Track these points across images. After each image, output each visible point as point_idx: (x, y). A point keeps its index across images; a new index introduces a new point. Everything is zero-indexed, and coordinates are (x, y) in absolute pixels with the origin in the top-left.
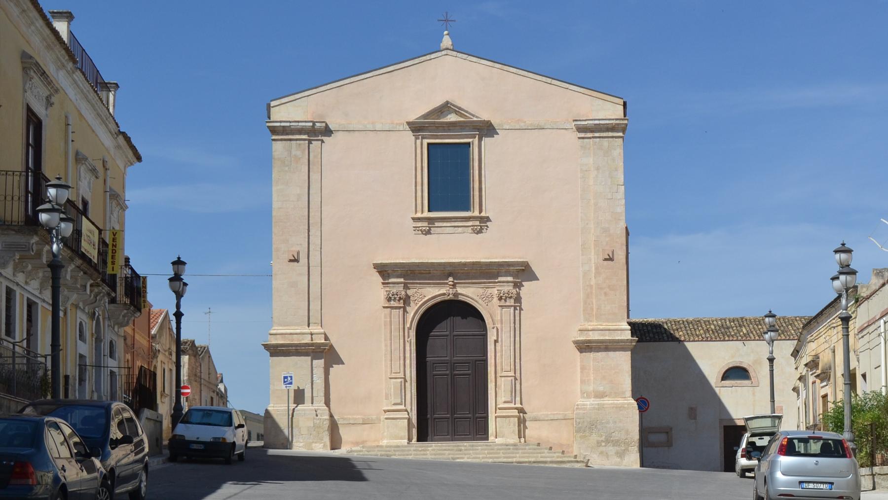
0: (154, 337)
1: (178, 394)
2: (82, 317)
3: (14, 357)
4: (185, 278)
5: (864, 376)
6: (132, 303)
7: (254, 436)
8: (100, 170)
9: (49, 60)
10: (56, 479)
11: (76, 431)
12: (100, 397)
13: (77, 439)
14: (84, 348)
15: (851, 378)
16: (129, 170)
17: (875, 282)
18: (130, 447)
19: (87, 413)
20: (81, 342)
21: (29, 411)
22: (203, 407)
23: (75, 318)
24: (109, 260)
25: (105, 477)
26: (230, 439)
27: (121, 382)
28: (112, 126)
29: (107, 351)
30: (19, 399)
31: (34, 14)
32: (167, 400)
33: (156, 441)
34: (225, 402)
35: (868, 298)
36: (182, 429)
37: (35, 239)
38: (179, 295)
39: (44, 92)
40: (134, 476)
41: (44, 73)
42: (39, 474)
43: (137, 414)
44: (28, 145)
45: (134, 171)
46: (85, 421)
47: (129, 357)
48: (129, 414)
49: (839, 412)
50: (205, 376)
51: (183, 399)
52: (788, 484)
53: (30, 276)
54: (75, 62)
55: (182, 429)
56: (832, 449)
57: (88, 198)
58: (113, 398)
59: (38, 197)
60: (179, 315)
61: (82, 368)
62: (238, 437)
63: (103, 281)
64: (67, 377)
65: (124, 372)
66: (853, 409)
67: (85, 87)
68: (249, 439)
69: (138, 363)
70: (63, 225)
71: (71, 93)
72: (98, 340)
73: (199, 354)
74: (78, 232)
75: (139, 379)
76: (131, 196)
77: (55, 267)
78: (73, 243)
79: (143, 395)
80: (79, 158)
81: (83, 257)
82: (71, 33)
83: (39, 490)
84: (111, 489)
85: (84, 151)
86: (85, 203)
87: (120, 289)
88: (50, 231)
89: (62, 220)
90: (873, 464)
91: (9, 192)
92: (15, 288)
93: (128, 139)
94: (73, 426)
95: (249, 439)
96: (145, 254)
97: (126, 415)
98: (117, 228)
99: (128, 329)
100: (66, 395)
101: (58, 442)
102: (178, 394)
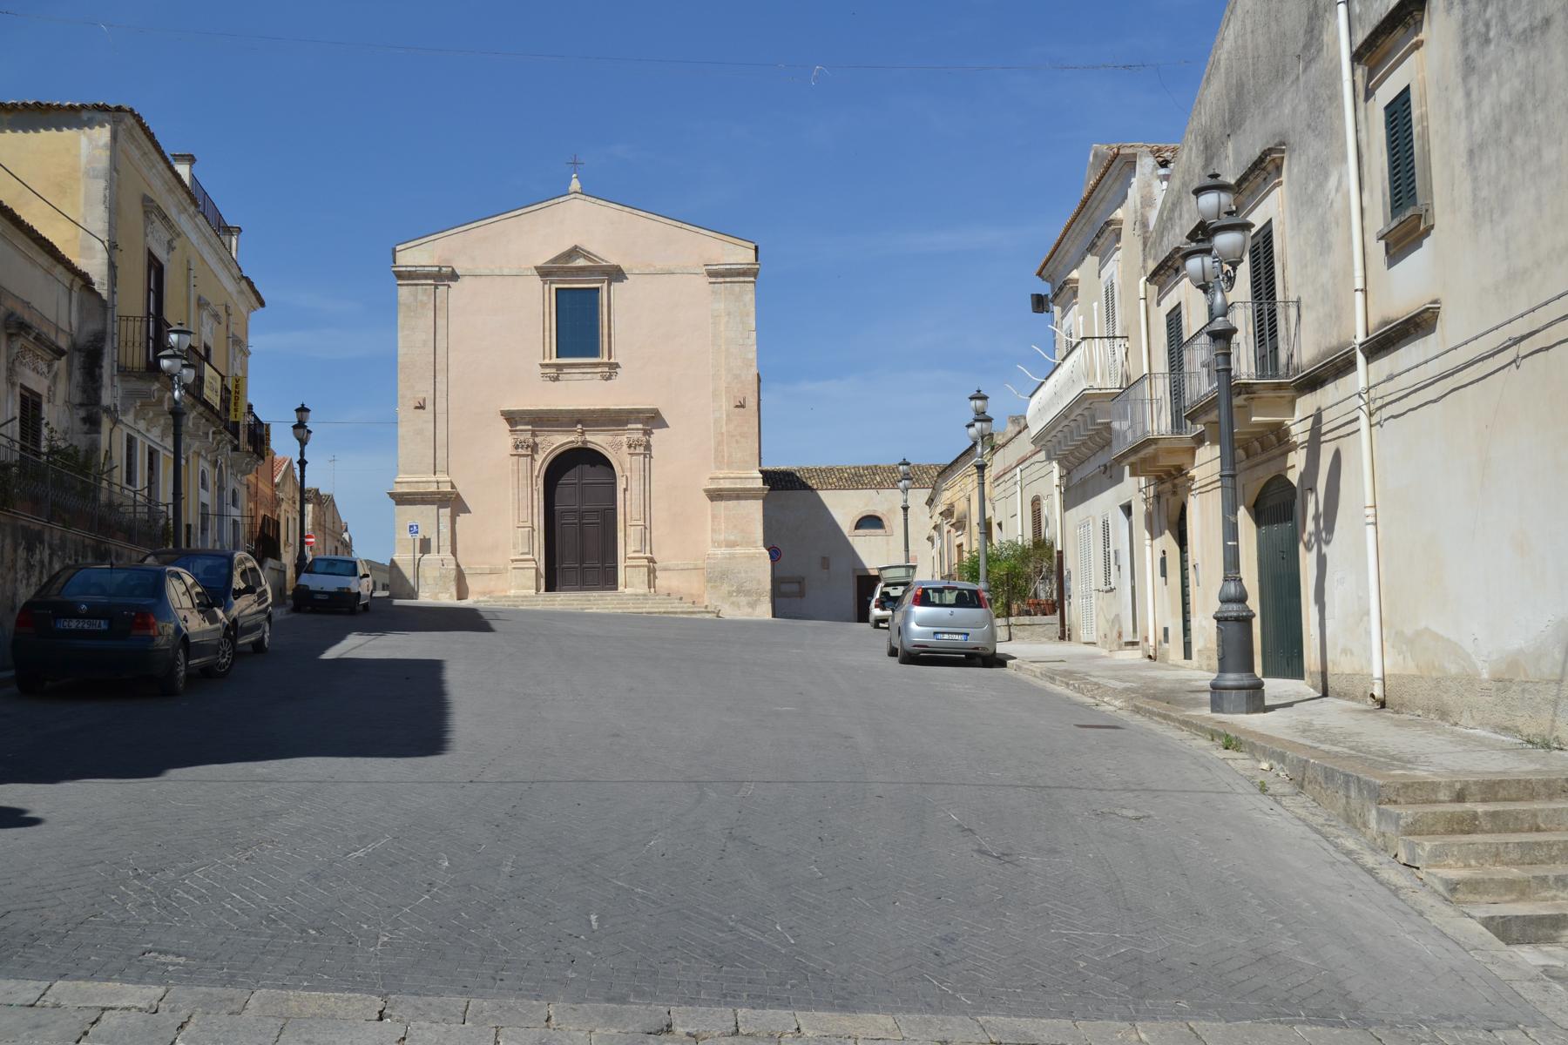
0: (277, 485)
1: (302, 544)
2: (204, 465)
3: (135, 506)
4: (309, 425)
5: (1000, 525)
6: (255, 451)
7: (379, 586)
8: (221, 317)
9: (171, 204)
10: (178, 630)
11: (199, 580)
12: (222, 546)
13: (199, 589)
14: (207, 497)
15: (986, 528)
16: (252, 315)
17: (1011, 429)
18: (254, 597)
19: (209, 562)
20: (204, 491)
21: (150, 560)
22: (328, 556)
23: (197, 466)
24: (232, 407)
25: (227, 628)
26: (354, 588)
27: (243, 531)
28: (235, 271)
29: (230, 500)
30: (142, 549)
31: (155, 156)
32: (290, 549)
33: (279, 591)
34: (350, 553)
35: (1004, 446)
36: (305, 579)
37: (156, 386)
38: (303, 443)
39: (166, 236)
40: (257, 627)
41: (165, 217)
42: (161, 624)
43: (261, 563)
44: (149, 289)
45: (257, 317)
46: (207, 570)
47: (252, 505)
48: (252, 563)
49: (974, 562)
50: (329, 525)
51: (307, 548)
52: (922, 635)
53: (151, 424)
54: (197, 206)
55: (305, 579)
56: (967, 600)
57: (210, 343)
58: (236, 547)
59: (160, 343)
60: (302, 463)
61: (205, 517)
62: (363, 587)
63: (226, 428)
64: (188, 526)
65: (247, 521)
66: (988, 558)
67: (208, 231)
68: (375, 589)
69: (262, 512)
70: (185, 371)
71: (193, 237)
72: (221, 488)
73: (324, 502)
74: (200, 379)
75: (262, 528)
76: (255, 342)
77: (177, 414)
78: (195, 390)
79: (266, 544)
80: (202, 304)
81: (206, 404)
82: (192, 176)
83: (161, 642)
84: (233, 640)
85: (208, 297)
86: (207, 349)
87: (243, 437)
88: (171, 377)
89: (184, 366)
90: (1009, 615)
91: (130, 338)
92: (136, 435)
93: (251, 284)
94: (195, 575)
95: (375, 589)
96: (268, 402)
97: (249, 565)
98: (240, 374)
99: (251, 477)
100: (188, 544)
101: (180, 592)
102: (302, 544)
